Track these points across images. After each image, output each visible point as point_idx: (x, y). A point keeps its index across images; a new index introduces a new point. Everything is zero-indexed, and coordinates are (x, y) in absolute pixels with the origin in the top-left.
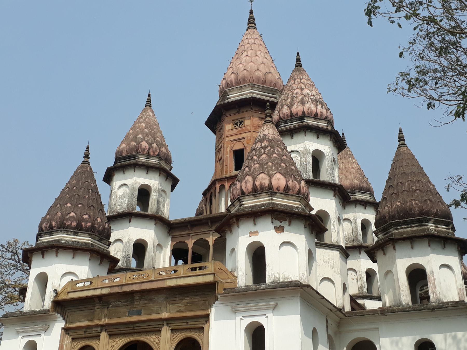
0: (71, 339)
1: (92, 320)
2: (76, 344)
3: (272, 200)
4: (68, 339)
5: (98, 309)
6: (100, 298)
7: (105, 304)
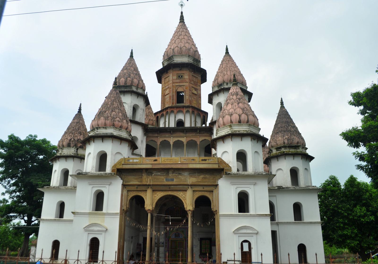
0: (127, 191)
1: (141, 182)
2: (130, 194)
3: (249, 128)
4: (125, 192)
5: (145, 176)
6: (147, 170)
7: (149, 173)
